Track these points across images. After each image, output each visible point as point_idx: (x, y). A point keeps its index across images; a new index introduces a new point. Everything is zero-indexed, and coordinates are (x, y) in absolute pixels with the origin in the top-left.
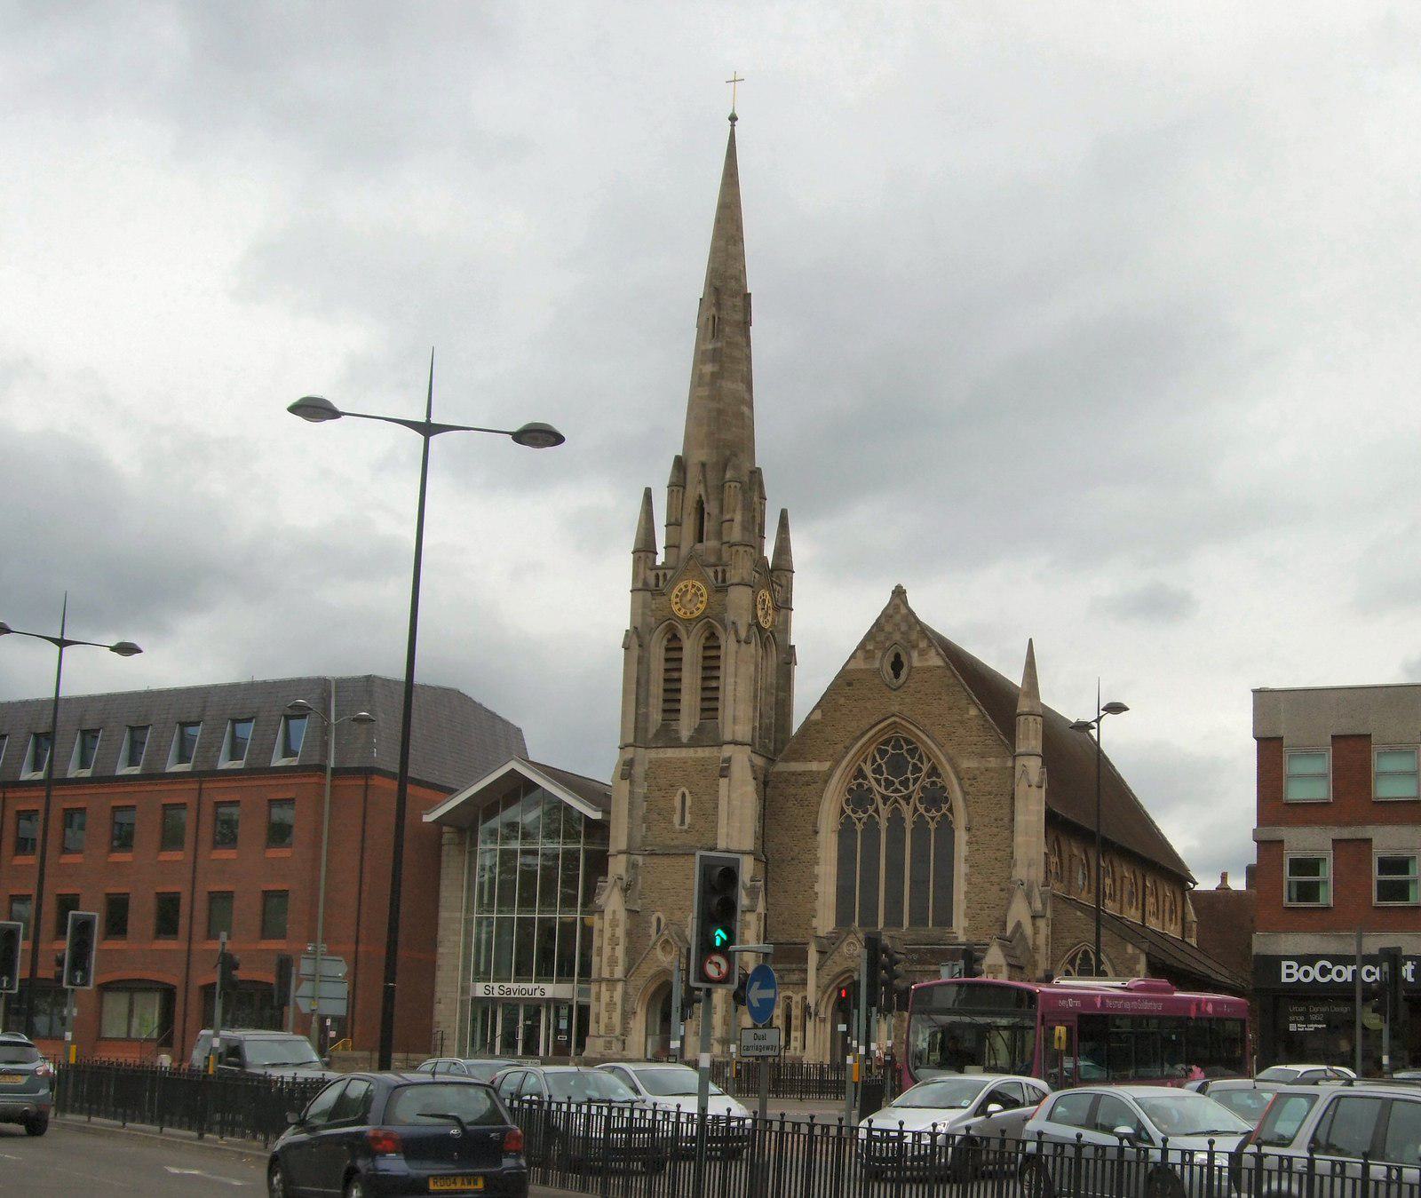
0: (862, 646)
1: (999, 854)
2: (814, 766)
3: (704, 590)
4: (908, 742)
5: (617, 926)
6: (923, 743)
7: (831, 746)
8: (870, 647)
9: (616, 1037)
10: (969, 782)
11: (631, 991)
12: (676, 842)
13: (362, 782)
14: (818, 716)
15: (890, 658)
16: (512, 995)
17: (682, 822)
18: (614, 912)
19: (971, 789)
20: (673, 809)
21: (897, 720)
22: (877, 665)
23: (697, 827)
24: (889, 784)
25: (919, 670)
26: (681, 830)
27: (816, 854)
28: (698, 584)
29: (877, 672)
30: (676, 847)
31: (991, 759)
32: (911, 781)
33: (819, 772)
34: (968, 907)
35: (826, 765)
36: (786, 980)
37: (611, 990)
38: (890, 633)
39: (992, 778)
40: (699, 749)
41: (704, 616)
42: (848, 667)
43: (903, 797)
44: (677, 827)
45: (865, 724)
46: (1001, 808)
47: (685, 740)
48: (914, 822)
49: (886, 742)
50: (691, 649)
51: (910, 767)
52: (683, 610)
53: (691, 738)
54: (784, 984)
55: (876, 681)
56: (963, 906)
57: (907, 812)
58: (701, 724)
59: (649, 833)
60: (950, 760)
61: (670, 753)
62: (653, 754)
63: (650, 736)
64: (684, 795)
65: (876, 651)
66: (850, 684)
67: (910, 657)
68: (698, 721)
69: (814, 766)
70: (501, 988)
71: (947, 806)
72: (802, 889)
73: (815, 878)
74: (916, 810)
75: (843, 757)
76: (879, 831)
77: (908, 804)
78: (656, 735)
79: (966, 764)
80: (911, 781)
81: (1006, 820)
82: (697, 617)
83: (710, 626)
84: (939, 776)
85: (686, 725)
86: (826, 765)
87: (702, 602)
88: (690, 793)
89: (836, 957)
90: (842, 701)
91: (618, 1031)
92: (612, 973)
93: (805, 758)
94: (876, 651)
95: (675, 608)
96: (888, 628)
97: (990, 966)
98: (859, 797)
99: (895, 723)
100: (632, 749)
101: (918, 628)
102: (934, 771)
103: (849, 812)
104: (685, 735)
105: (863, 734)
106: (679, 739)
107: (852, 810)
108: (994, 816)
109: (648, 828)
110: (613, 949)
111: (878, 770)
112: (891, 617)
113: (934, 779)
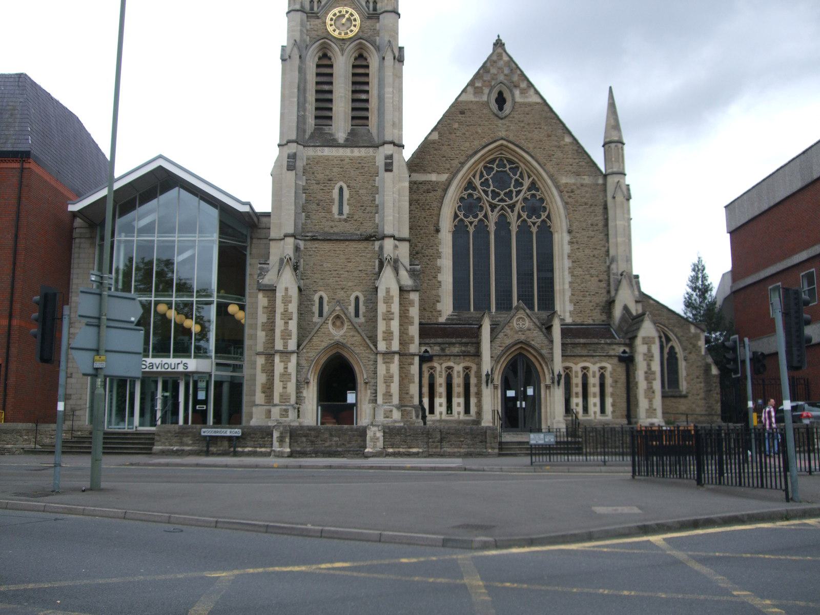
0: (471, 83)
1: (596, 252)
2: (433, 177)
3: (356, 16)
4: (510, 162)
5: (290, 302)
6: (526, 163)
7: (447, 161)
8: (478, 84)
9: (292, 405)
10: (567, 195)
11: (303, 362)
12: (336, 230)
13: (17, 165)
14: (436, 136)
15: (494, 95)
16: (155, 369)
17: (341, 212)
18: (286, 289)
19: (569, 200)
20: (332, 201)
21: (505, 143)
22: (485, 98)
23: (356, 217)
24: (495, 194)
26: (340, 219)
27: (438, 250)
28: (350, 10)
29: (487, 104)
30: (334, 234)
31: (583, 177)
32: (514, 194)
33: (437, 183)
34: (572, 295)
35: (444, 177)
36: (447, 352)
37: (286, 362)
38: (495, 75)
39: (587, 192)
40: (356, 150)
41: (357, 37)
42: (461, 99)
43: (509, 206)
44: (336, 216)
45: (477, 144)
46: (596, 216)
47: (341, 141)
48: (518, 226)
49: (492, 161)
50: (342, 66)
51: (513, 183)
52: (337, 31)
53: (347, 140)
54: (446, 355)
55: (485, 111)
56: (568, 294)
57: (513, 218)
58: (352, 130)
59: (309, 221)
60: (551, 177)
61: (327, 152)
62: (311, 152)
63: (307, 137)
64: (341, 189)
65: (484, 88)
66: (462, 113)
67: (513, 95)
68: (350, 127)
69: (433, 177)
71: (546, 214)
72: (426, 278)
73: (439, 270)
74: (519, 216)
75: (458, 171)
76: (488, 233)
77: (512, 211)
78: (312, 136)
79: (564, 180)
80: (514, 194)
81: (601, 224)
82: (350, 38)
83: (361, 47)
84: (537, 190)
85: (341, 126)
86: (444, 177)
87: (355, 26)
88: (348, 186)
89: (507, 330)
90: (456, 126)
91: (293, 400)
92: (286, 345)
93: (424, 170)
94: (484, 88)
95: (330, 29)
96: (493, 71)
97: (644, 338)
98: (469, 205)
99: (502, 145)
100: (295, 144)
101: (519, 72)
102: (533, 186)
103: (462, 216)
104: (341, 136)
105: (476, 153)
106: (335, 140)
107: (464, 215)
109: (308, 217)
111: (485, 183)
112: (495, 62)
113: (533, 192)
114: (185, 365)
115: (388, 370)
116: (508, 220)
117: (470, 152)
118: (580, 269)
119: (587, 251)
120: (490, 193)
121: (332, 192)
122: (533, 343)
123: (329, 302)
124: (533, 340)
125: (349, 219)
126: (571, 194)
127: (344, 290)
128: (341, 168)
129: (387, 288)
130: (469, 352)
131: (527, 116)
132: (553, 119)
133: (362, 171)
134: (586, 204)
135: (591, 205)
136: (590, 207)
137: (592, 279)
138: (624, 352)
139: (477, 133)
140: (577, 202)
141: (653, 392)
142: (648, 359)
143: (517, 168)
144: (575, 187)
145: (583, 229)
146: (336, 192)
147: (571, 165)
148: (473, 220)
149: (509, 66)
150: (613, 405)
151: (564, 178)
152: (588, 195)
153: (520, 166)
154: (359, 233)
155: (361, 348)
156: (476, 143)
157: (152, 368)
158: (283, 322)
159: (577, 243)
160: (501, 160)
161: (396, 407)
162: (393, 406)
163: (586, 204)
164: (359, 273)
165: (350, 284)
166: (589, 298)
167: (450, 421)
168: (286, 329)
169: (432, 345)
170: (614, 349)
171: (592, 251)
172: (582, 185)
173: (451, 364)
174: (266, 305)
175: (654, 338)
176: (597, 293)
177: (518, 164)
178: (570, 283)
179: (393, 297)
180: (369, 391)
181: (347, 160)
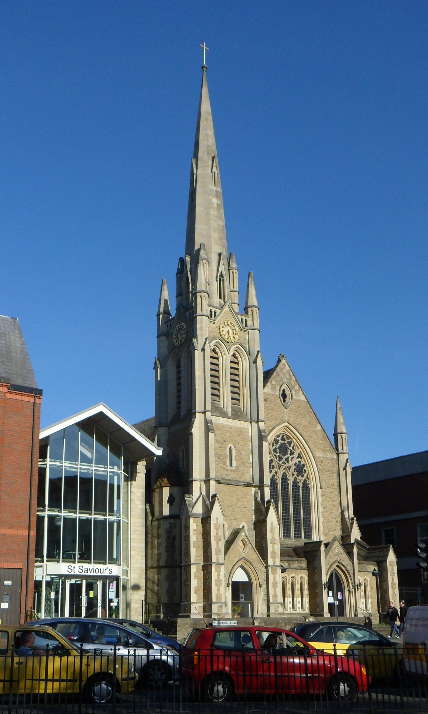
1: (334, 503)
4: (288, 438)
13: (32, 400)
16: (89, 574)
17: (231, 465)
18: (217, 519)
19: (321, 467)
23: (240, 469)
24: (280, 458)
25: (296, 400)
26: (231, 469)
46: (333, 479)
65: (277, 386)
70: (81, 568)
74: (293, 475)
79: (319, 454)
81: (336, 484)
88: (235, 447)
94: (277, 386)
108: (331, 483)
110: (218, 543)
113: (299, 459)
114: (110, 571)
115: (274, 578)
116: (288, 477)
117: (271, 428)
118: (327, 513)
119: (330, 502)
120: (277, 457)
121: (226, 450)
122: (343, 562)
123: (228, 528)
124: (343, 561)
125: (236, 470)
126: (321, 464)
127: (237, 521)
128: (230, 433)
129: (271, 522)
130: (302, 567)
131: (299, 408)
132: (311, 413)
133: (242, 437)
134: (329, 471)
135: (331, 472)
136: (330, 473)
137: (333, 520)
138: (375, 570)
139: (274, 415)
140: (324, 468)
141: (395, 595)
142: (393, 575)
143: (291, 442)
144: (323, 459)
145: (327, 487)
146: (228, 450)
147: (321, 444)
148: (301, 478)
149: (289, 373)
150: (371, 604)
151: (318, 453)
152: (329, 465)
153: (293, 441)
154: (242, 480)
155: (257, 563)
156: (273, 422)
157: (87, 572)
158: (216, 542)
159: (325, 496)
160: (283, 436)
161: (281, 605)
162: (278, 603)
163: (329, 471)
164: (244, 509)
165: (240, 517)
166: (332, 533)
167: (296, 614)
168: (218, 547)
169: (284, 562)
170: (370, 568)
171: (332, 502)
172: (326, 458)
173: (293, 575)
174: (195, 528)
175: (394, 562)
176: (336, 529)
177: (292, 439)
178: (323, 522)
179: (275, 528)
180: (262, 593)
181: (233, 429)
